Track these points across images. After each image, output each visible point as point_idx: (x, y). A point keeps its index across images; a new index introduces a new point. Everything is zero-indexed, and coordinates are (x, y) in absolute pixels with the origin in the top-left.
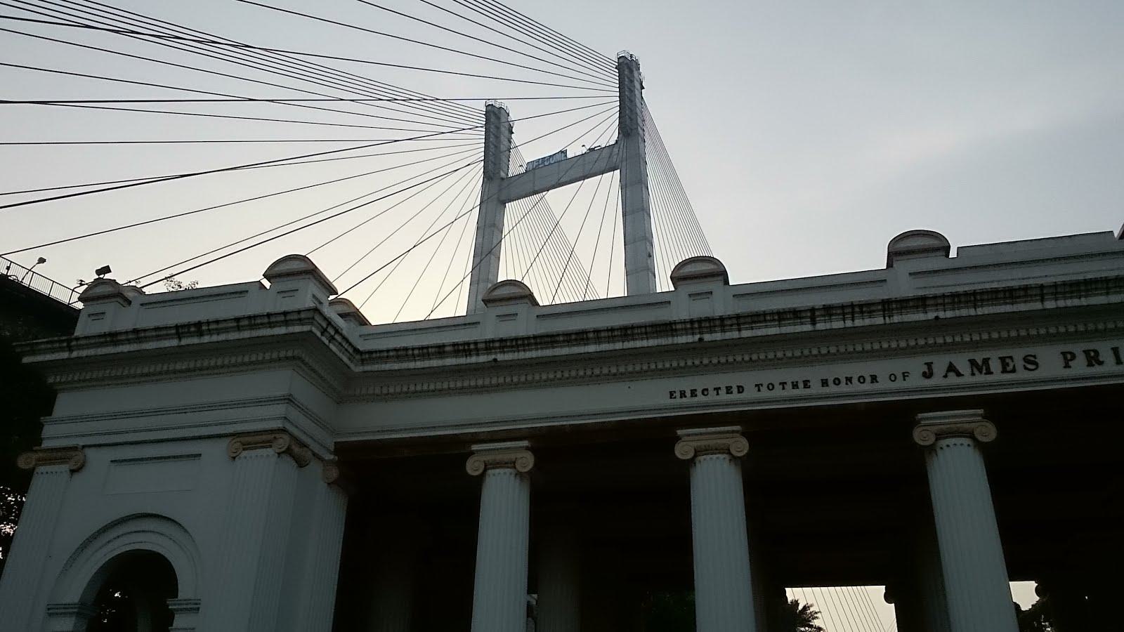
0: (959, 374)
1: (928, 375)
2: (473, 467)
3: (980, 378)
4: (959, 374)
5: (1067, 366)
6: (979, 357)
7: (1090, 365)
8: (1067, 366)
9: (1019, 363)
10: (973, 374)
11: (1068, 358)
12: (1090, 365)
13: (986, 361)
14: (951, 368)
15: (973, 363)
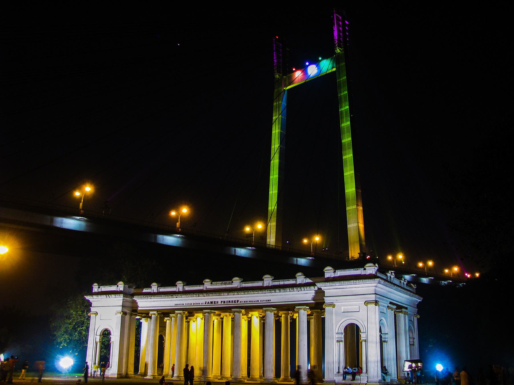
0: (209, 304)
1: (205, 303)
2: (150, 315)
3: (211, 304)
4: (209, 304)
5: (221, 303)
6: (212, 301)
7: (224, 303)
8: (221, 303)
9: (216, 302)
10: (211, 304)
11: (222, 302)
12: (224, 303)
13: (213, 302)
14: (208, 303)
15: (211, 302)
